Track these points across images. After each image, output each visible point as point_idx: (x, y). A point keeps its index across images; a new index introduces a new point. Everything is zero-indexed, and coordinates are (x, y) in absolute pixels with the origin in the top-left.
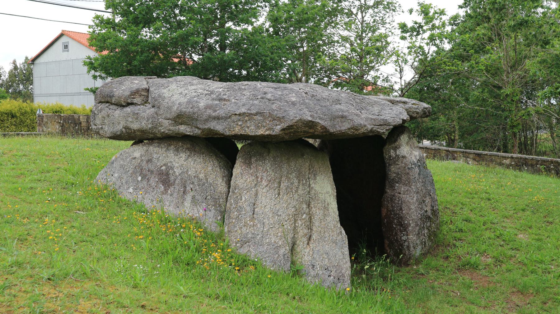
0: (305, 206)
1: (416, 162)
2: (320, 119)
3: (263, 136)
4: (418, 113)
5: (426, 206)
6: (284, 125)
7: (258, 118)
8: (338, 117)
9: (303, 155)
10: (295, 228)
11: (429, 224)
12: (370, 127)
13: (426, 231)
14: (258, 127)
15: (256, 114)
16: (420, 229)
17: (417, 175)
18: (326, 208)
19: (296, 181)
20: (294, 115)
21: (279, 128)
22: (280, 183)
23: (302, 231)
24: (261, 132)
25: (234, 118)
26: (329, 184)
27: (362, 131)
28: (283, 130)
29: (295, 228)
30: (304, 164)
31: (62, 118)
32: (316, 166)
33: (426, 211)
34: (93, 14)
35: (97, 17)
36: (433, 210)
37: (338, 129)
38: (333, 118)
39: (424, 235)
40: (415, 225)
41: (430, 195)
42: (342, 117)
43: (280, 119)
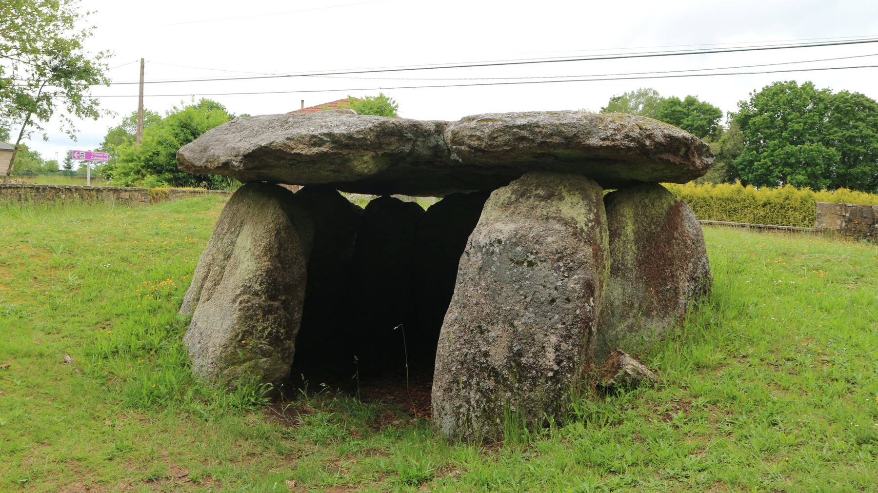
1: (482, 244)
4: (479, 138)
5: (488, 344)
11: (490, 384)
13: (474, 396)
16: (456, 381)
23: (208, 284)
26: (250, 238)
31: (850, 209)
33: (486, 354)
36: (519, 365)
39: (468, 401)
40: (443, 368)
41: (512, 325)
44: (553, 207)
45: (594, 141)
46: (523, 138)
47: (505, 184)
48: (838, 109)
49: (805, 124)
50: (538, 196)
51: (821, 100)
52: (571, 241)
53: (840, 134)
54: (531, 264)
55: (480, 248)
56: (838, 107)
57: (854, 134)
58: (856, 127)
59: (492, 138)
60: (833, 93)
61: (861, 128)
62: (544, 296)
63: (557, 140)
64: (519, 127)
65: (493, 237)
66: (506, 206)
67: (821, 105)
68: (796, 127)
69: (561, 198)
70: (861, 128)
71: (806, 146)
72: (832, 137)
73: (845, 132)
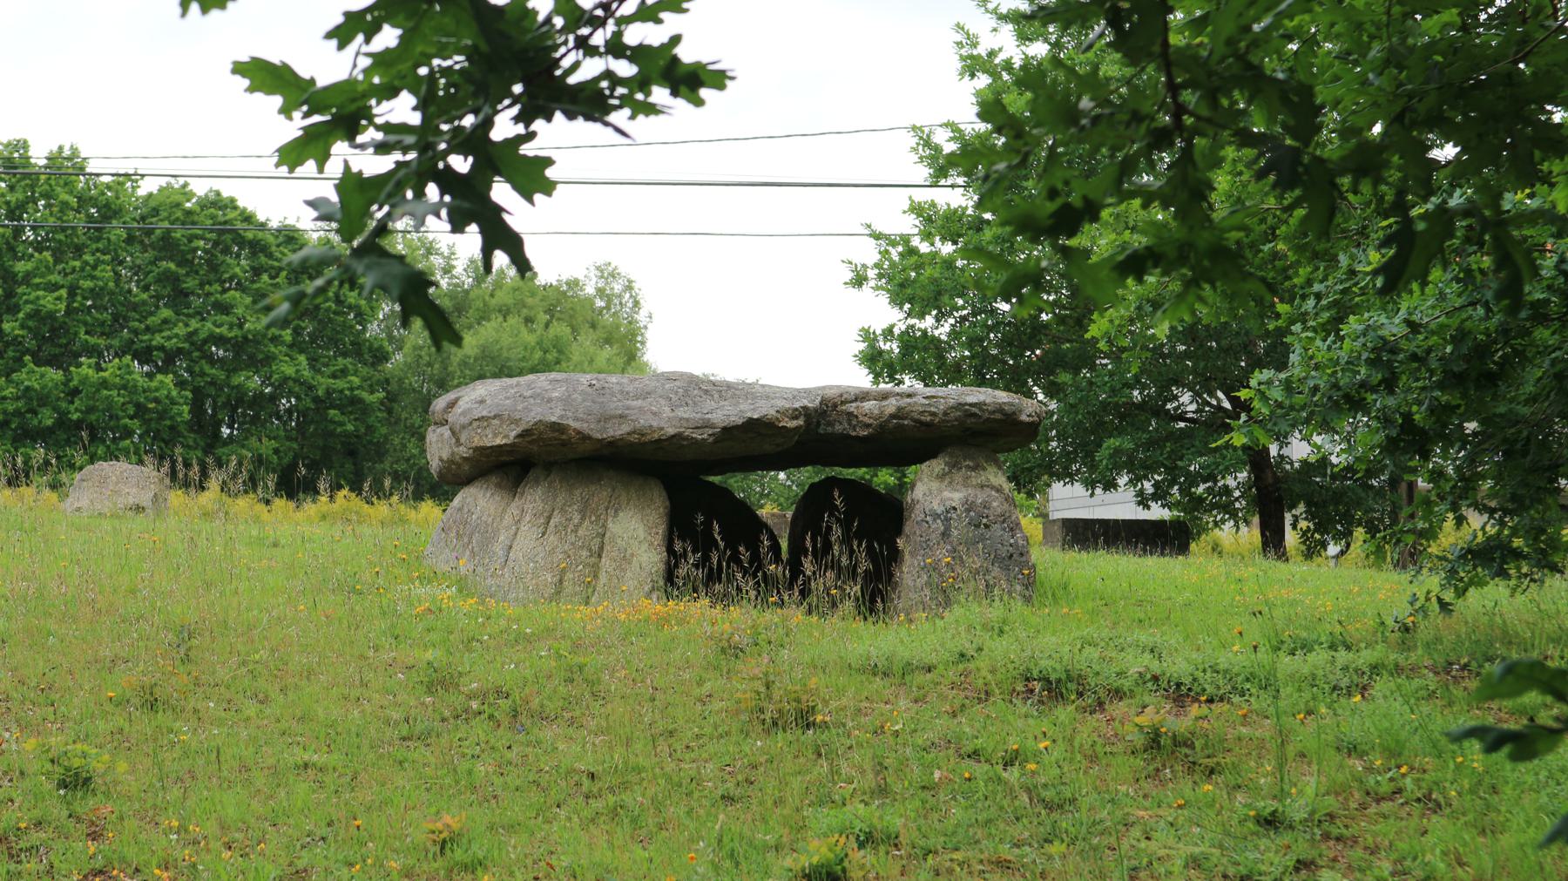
0: (585, 553)
2: (576, 419)
3: (500, 446)
4: (933, 414)
6: (519, 430)
7: (496, 422)
8: (614, 417)
9: (600, 480)
10: (561, 581)
12: (671, 431)
14: (495, 435)
15: (495, 417)
17: (935, 537)
18: (626, 559)
19: (576, 518)
20: (537, 413)
21: (513, 434)
22: (549, 518)
24: (498, 441)
25: (475, 424)
27: (656, 436)
28: (518, 436)
29: (561, 581)
30: (600, 494)
32: (623, 498)
34: (901, 198)
35: (916, 209)
37: (611, 433)
38: (607, 419)
42: (621, 416)
43: (517, 422)
44: (981, 477)
45: (1024, 418)
46: (974, 415)
47: (934, 456)
48: (167, 246)
49: (72, 292)
50: (968, 467)
51: (110, 211)
52: (1006, 506)
53: (180, 330)
54: (987, 526)
55: (939, 516)
56: (166, 236)
57: (223, 330)
58: (225, 309)
59: (945, 414)
60: (142, 192)
61: (239, 311)
62: (1003, 552)
63: (998, 416)
64: (971, 405)
65: (948, 504)
66: (941, 477)
67: (116, 231)
68: (53, 303)
69: (984, 469)
70: (239, 311)
71: (85, 369)
72: (158, 340)
73: (194, 324)
